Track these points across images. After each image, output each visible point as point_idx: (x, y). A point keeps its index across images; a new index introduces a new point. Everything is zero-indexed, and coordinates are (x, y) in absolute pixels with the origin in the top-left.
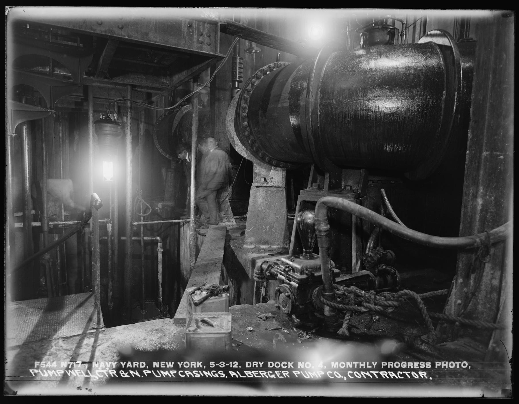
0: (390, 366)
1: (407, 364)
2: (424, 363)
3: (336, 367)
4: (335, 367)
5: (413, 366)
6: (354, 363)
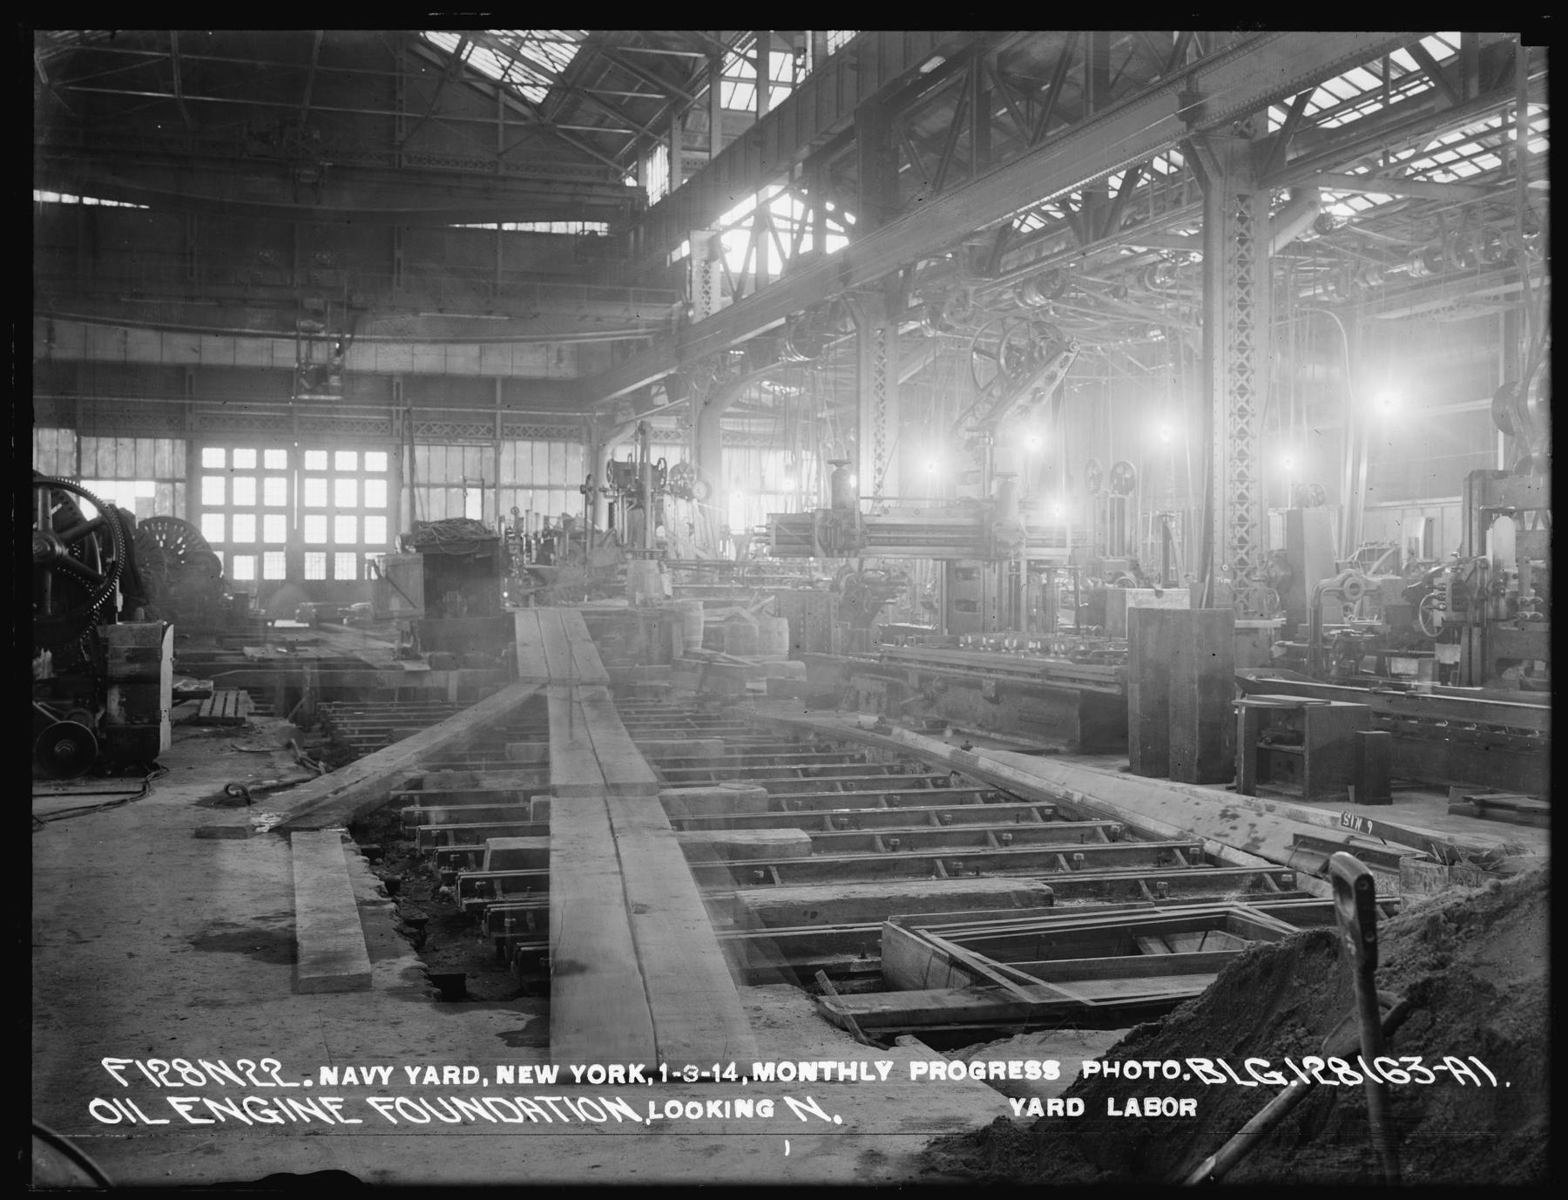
0: (937, 1076)
1: (987, 1069)
2: (1038, 1064)
3: (768, 1081)
4: (764, 1079)
5: (1007, 1073)
6: (822, 1065)
